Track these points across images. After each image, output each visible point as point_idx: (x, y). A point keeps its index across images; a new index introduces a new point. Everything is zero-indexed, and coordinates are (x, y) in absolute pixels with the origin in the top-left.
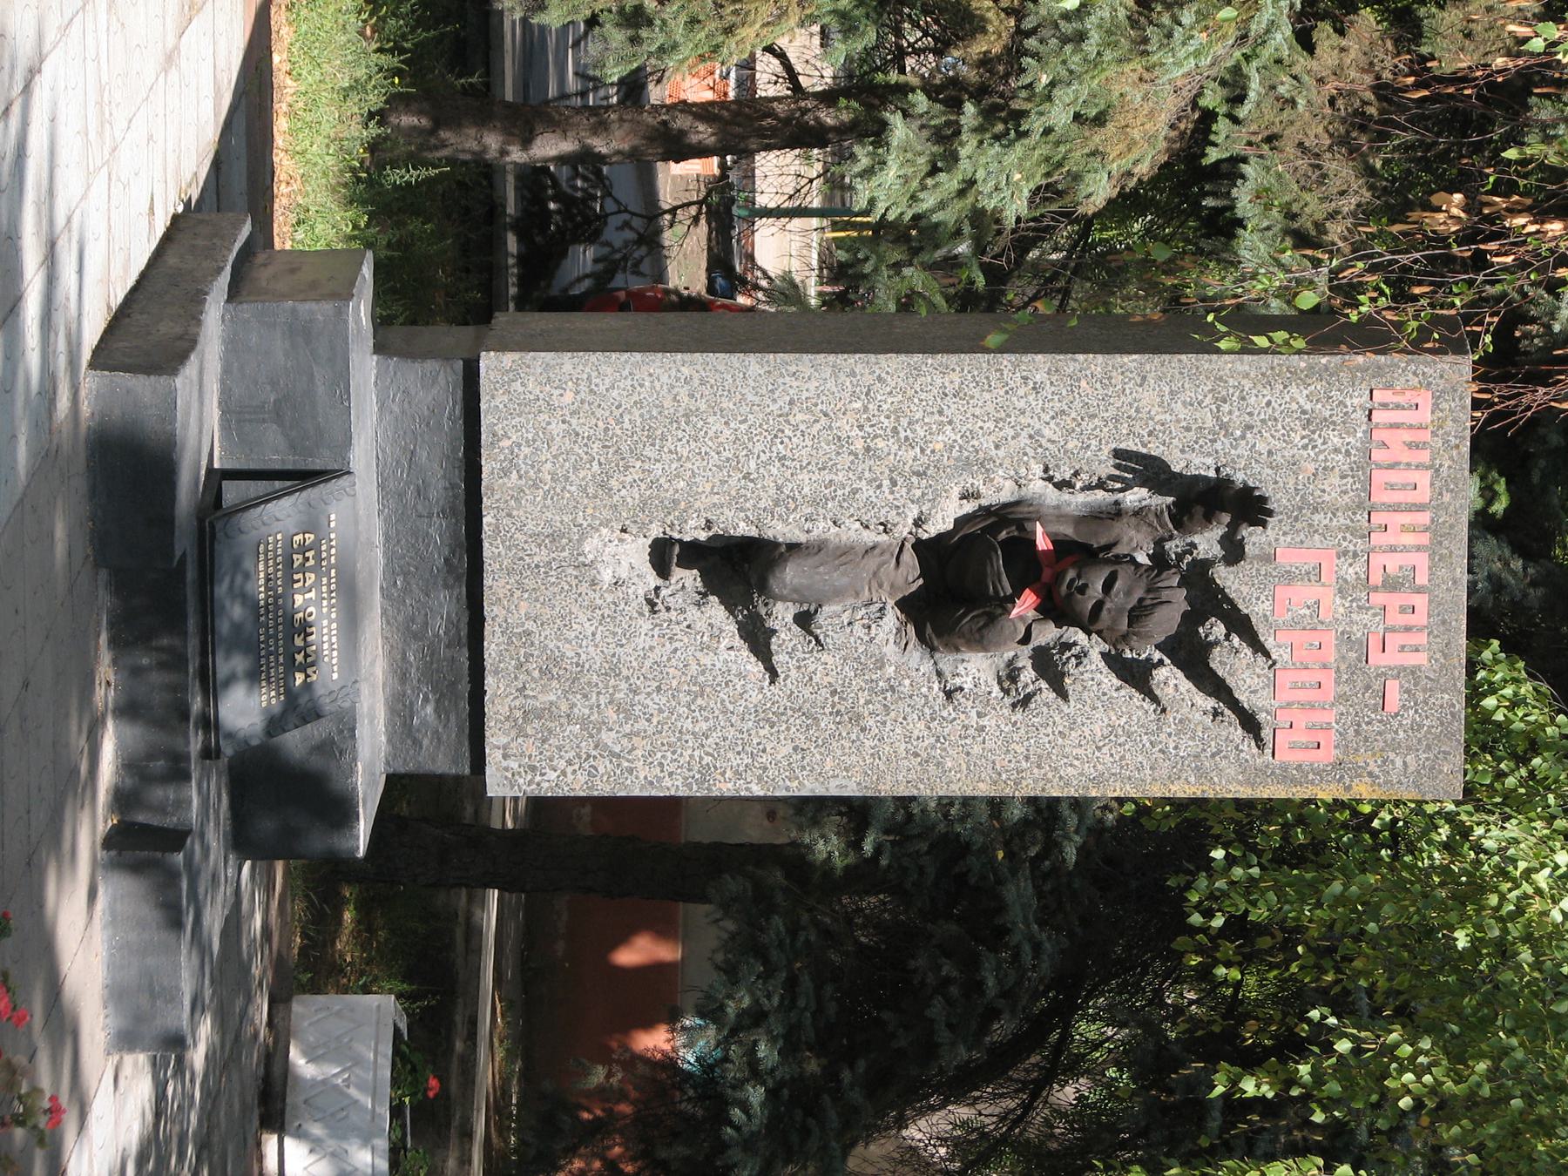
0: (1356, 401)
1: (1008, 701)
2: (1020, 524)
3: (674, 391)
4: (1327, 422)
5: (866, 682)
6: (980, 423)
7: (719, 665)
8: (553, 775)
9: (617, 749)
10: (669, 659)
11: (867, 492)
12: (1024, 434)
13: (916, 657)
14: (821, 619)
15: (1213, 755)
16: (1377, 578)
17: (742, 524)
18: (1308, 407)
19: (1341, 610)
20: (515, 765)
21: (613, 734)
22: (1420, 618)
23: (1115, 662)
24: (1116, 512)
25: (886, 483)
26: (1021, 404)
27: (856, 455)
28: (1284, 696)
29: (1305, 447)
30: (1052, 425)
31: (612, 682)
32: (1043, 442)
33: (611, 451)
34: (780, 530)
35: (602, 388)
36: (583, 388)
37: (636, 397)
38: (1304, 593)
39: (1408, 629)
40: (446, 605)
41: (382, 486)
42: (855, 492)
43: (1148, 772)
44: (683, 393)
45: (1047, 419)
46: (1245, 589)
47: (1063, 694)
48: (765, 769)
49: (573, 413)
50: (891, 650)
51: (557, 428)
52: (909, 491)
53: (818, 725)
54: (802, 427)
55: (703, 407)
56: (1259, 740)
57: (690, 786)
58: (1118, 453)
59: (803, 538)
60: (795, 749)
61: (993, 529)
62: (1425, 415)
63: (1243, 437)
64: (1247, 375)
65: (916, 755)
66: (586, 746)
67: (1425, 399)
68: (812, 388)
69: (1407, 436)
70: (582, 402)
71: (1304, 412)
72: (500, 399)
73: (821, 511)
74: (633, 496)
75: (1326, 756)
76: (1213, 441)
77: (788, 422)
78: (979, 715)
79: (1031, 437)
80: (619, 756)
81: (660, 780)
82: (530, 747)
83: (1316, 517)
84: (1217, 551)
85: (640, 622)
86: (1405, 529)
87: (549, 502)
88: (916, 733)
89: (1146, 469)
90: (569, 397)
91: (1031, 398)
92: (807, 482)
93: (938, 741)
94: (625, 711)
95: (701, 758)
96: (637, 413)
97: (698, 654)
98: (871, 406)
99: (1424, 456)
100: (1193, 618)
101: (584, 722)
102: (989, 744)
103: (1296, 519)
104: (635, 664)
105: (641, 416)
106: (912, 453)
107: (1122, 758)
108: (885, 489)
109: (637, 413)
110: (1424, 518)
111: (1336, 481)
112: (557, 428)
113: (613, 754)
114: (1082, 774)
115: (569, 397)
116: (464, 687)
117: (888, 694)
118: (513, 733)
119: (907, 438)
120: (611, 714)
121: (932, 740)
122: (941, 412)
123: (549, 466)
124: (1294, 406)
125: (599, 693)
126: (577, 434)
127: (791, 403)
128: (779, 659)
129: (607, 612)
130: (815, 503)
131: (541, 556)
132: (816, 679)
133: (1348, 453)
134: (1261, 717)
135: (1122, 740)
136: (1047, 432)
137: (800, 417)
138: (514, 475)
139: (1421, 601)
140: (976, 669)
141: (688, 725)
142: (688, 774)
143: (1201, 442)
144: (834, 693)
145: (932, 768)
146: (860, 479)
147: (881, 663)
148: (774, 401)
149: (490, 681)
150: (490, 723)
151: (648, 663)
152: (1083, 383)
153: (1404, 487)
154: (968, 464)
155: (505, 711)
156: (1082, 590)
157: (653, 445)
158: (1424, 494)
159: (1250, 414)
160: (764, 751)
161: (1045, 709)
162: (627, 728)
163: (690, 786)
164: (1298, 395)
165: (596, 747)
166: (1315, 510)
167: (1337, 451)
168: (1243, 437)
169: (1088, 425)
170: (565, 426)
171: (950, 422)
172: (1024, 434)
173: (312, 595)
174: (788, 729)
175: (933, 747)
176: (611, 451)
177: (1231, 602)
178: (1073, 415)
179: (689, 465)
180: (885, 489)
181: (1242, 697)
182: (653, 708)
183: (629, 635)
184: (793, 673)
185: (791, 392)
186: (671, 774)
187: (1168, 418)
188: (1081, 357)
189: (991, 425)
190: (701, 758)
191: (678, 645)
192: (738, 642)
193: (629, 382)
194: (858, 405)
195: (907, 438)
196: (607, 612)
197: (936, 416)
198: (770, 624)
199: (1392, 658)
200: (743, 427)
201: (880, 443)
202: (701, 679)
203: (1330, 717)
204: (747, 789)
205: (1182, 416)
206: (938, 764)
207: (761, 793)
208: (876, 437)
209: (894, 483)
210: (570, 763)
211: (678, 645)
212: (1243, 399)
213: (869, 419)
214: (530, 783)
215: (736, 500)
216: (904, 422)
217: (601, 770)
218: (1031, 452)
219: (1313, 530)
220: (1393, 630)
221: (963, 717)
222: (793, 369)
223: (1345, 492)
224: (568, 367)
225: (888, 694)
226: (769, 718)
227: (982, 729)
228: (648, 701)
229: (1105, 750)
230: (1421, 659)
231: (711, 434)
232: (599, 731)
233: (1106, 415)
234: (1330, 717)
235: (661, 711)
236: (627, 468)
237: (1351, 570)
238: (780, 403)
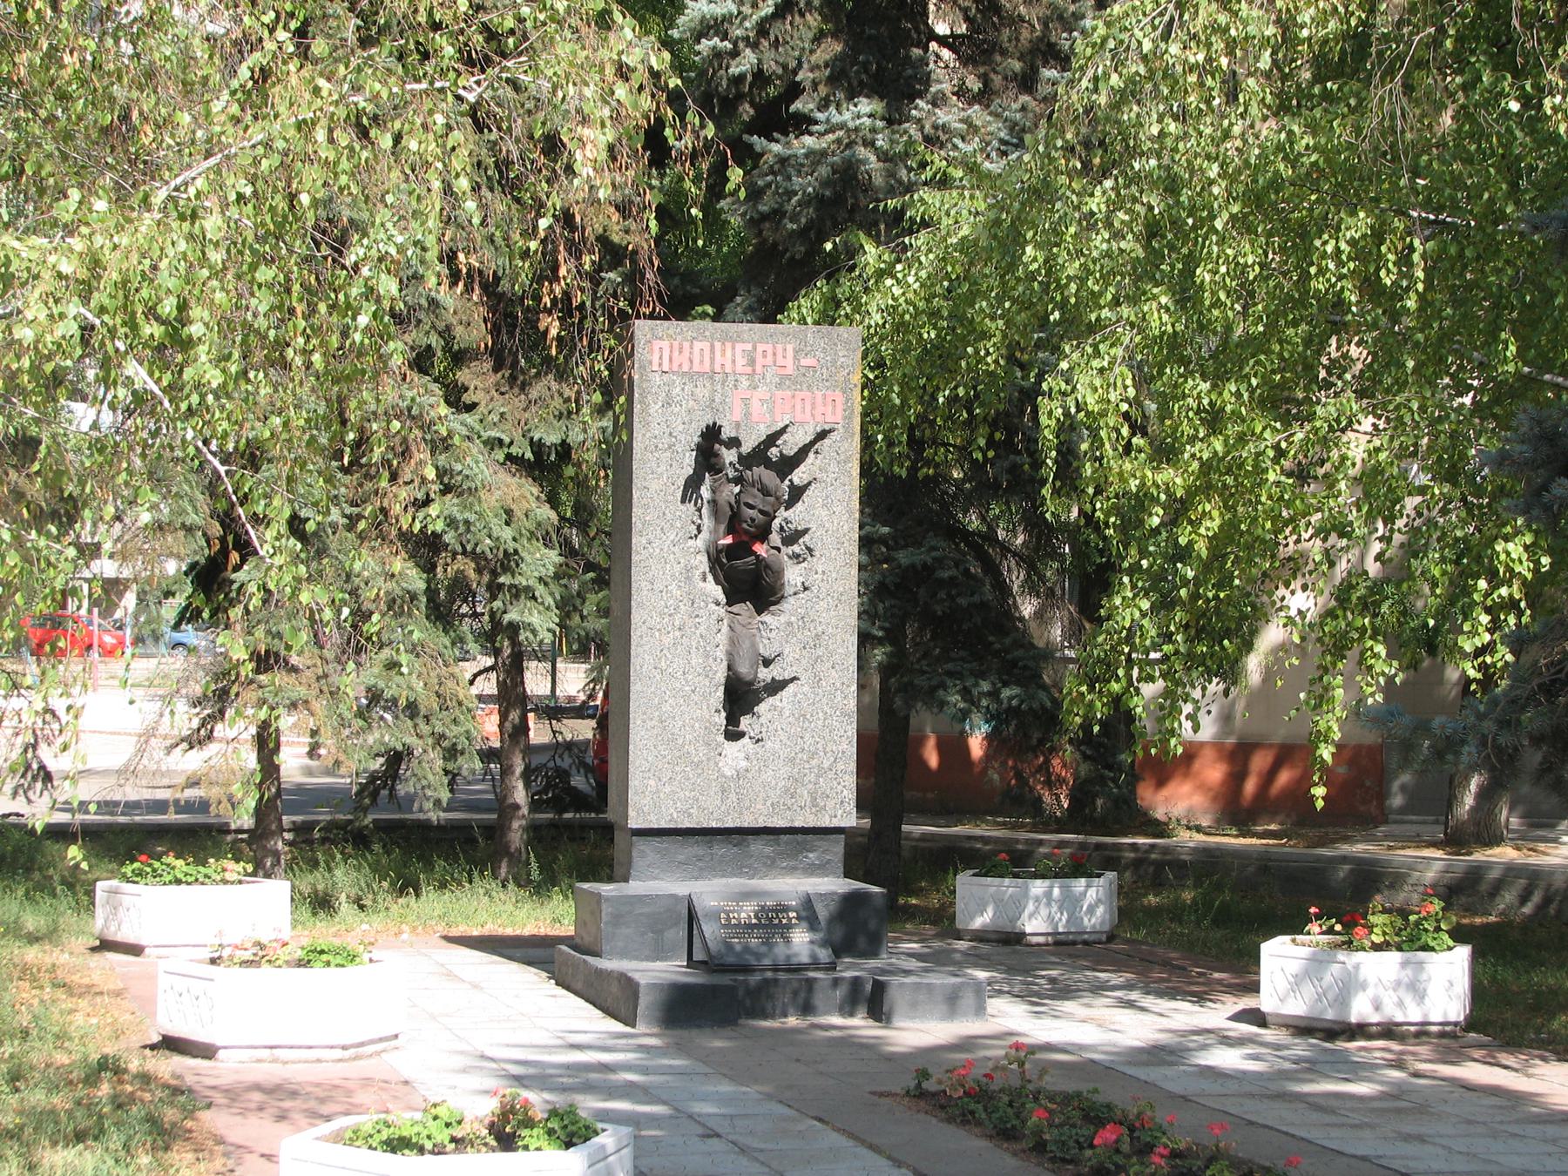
2: (719, 552)
11: (702, 629)
14: (766, 654)
16: (749, 370)
22: (769, 348)
23: (790, 504)
24: (713, 503)
34: (721, 675)
38: (756, 408)
40: (757, 846)
41: (697, 879)
44: (650, 724)
47: (806, 531)
50: (783, 619)
51: (667, 789)
56: (830, 431)
58: (683, 501)
59: (725, 663)
61: (721, 565)
62: (665, 344)
66: (831, 775)
67: (657, 344)
69: (676, 353)
72: (652, 817)
74: (703, 750)
75: (839, 396)
82: (830, 804)
84: (734, 451)
86: (723, 355)
89: (691, 487)
90: (652, 782)
92: (696, 660)
94: (813, 755)
99: (686, 345)
100: (768, 464)
101: (818, 776)
110: (718, 345)
112: (667, 789)
115: (652, 782)
116: (800, 837)
120: (814, 762)
130: (707, 656)
131: (733, 797)
134: (819, 429)
140: (793, 575)
147: (790, 624)
149: (797, 824)
150: (819, 824)
154: (688, 578)
156: (753, 520)
158: (706, 345)
164: (654, 408)
169: (669, 516)
192: (778, 697)
198: (769, 680)
199: (789, 362)
203: (819, 394)
219: (723, 402)
230: (790, 348)
234: (819, 394)
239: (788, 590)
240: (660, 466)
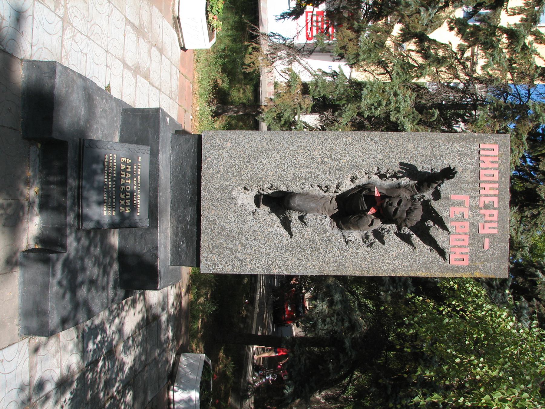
0: (475, 148)
1: (365, 245)
2: (369, 189)
4: (466, 155)
5: (321, 237)
11: (322, 175)
12: (371, 157)
13: (336, 231)
14: (307, 217)
15: (430, 263)
16: (482, 205)
17: (282, 186)
18: (460, 149)
19: (471, 215)
20: (209, 263)
21: (240, 254)
22: (495, 218)
23: (398, 234)
24: (399, 186)
25: (328, 172)
26: (371, 148)
27: (318, 164)
28: (453, 243)
29: (459, 163)
32: (377, 160)
34: (294, 188)
37: (250, 145)
38: (458, 210)
39: (491, 222)
40: (190, 213)
41: (172, 174)
42: (318, 175)
43: (410, 268)
44: (264, 143)
45: (379, 152)
46: (441, 208)
47: (383, 242)
50: (328, 227)
51: (225, 154)
53: (305, 252)
54: (302, 154)
55: (271, 148)
56: (445, 258)
58: (401, 164)
59: (301, 191)
60: (298, 259)
61: (361, 192)
62: (496, 153)
63: (440, 159)
64: (441, 139)
65: (336, 262)
66: (232, 257)
67: (496, 147)
69: (491, 159)
71: (459, 151)
72: (208, 145)
74: (248, 176)
75: (466, 263)
76: (431, 160)
77: (297, 153)
78: (357, 249)
79: (374, 158)
80: (242, 261)
81: (255, 269)
83: (463, 185)
84: (431, 197)
87: (222, 178)
88: (336, 254)
89: (410, 170)
90: (229, 145)
92: (303, 172)
93: (343, 257)
94: (244, 246)
96: (250, 150)
99: (496, 166)
100: (424, 219)
101: (231, 250)
102: (359, 259)
103: (457, 185)
106: (336, 163)
107: (402, 263)
108: (327, 174)
109: (250, 150)
110: (496, 186)
111: (469, 173)
112: (225, 154)
113: (240, 260)
114: (389, 269)
116: (195, 238)
118: (209, 252)
119: (334, 158)
120: (240, 247)
121: (341, 257)
122: (345, 150)
123: (222, 166)
124: (456, 149)
128: (293, 230)
129: (239, 214)
130: (305, 179)
131: (219, 195)
132: (305, 236)
133: (472, 165)
134: (446, 250)
136: (378, 156)
137: (301, 151)
138: (212, 169)
139: (495, 213)
140: (355, 235)
144: (310, 241)
145: (341, 266)
147: (325, 231)
148: (293, 146)
149: (202, 235)
150: (202, 249)
151: (251, 231)
152: (390, 141)
153: (490, 175)
155: (206, 245)
156: (391, 204)
158: (496, 178)
159: (442, 152)
162: (245, 252)
163: (264, 271)
164: (457, 146)
166: (462, 183)
167: (469, 164)
168: (440, 159)
171: (348, 153)
172: (371, 157)
174: (296, 253)
175: (342, 259)
177: (436, 212)
180: (327, 174)
181: (440, 244)
182: (253, 245)
183: (246, 221)
184: (298, 234)
186: (258, 267)
188: (389, 133)
189: (361, 154)
192: (280, 225)
193: (248, 140)
194: (319, 147)
195: (334, 158)
196: (239, 214)
198: (291, 219)
199: (487, 231)
201: (326, 160)
206: (343, 265)
207: (287, 274)
208: (325, 157)
209: (330, 173)
210: (226, 263)
212: (440, 147)
215: (281, 178)
216: (334, 153)
217: (236, 265)
218: (374, 163)
220: (487, 222)
222: (299, 136)
223: (472, 177)
224: (229, 135)
226: (290, 249)
228: (251, 243)
229: (396, 261)
230: (495, 231)
231: (273, 156)
232: (236, 252)
234: (467, 250)
235: (256, 246)
237: (474, 203)
239: (346, 233)
240: (425, 149)
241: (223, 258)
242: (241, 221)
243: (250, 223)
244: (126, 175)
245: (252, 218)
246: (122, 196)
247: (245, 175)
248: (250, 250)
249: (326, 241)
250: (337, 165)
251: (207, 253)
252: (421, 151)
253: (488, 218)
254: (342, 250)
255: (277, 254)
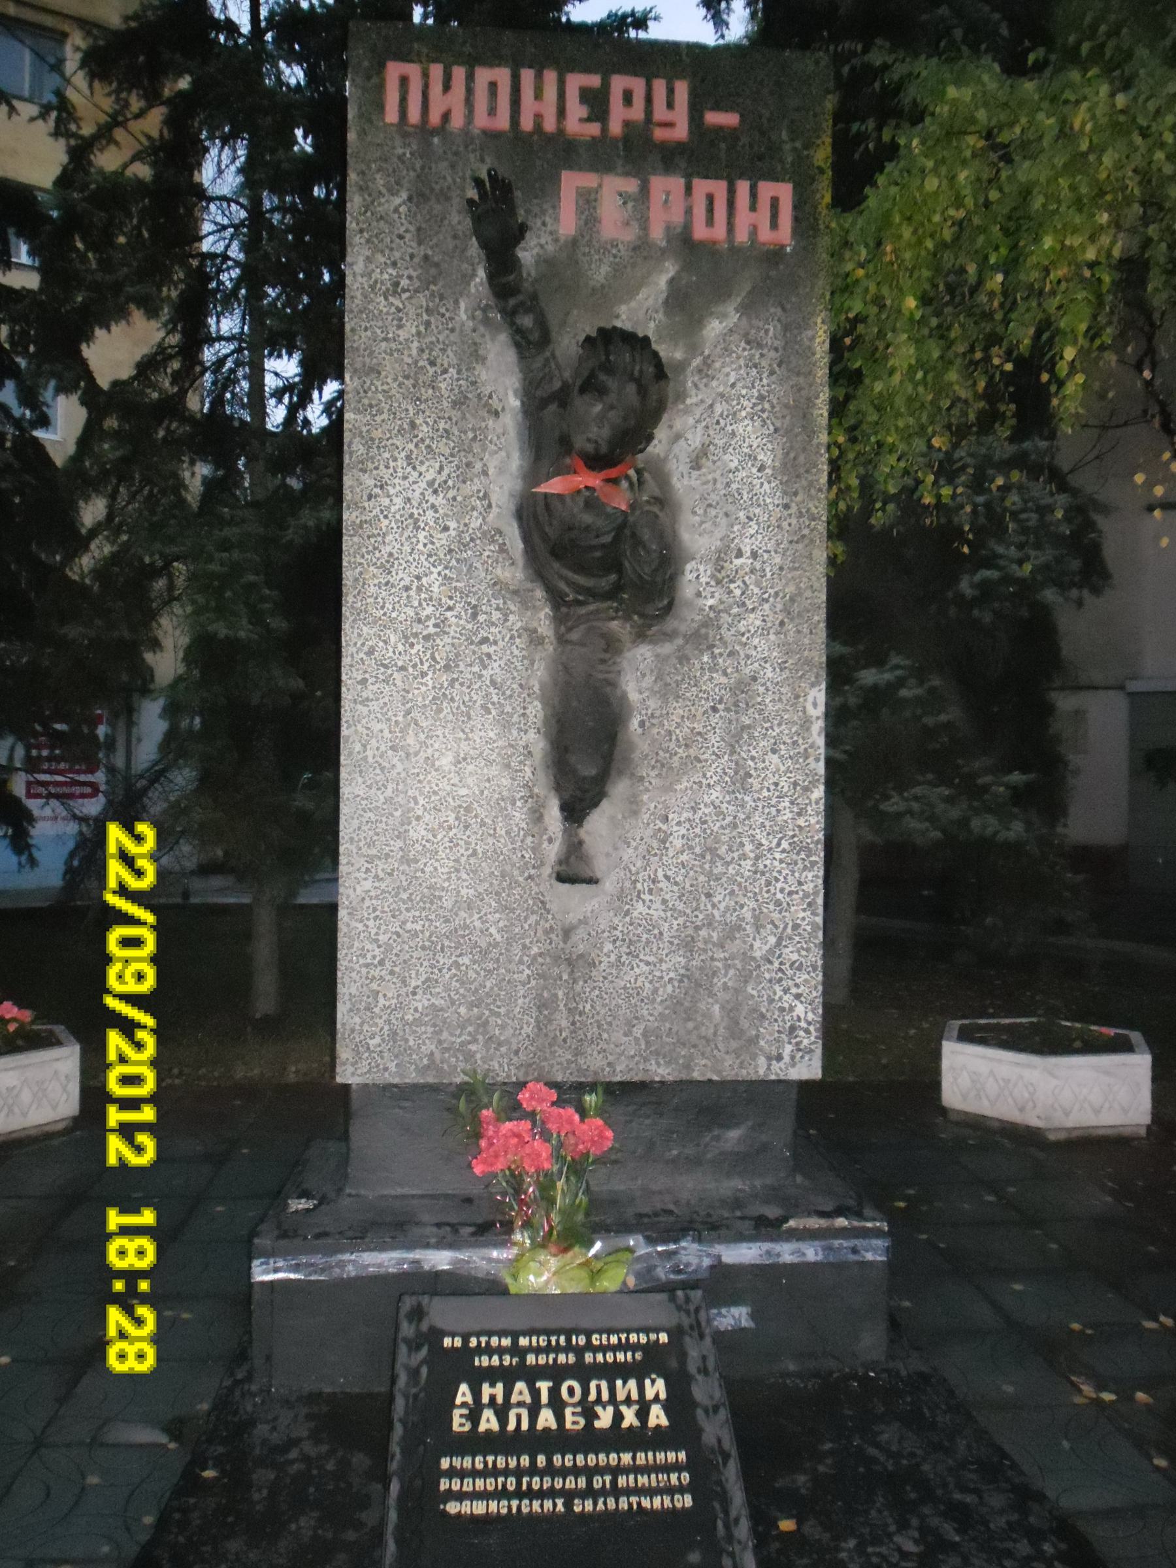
3: (381, 875)
6: (420, 546)
7: (683, 831)
8: (800, 1009)
9: (772, 940)
10: (676, 884)
11: (494, 669)
16: (594, 129)
20: (788, 1049)
21: (757, 944)
22: (637, 85)
25: (485, 648)
26: (398, 501)
27: (453, 681)
30: (423, 469)
31: (701, 945)
33: (447, 943)
35: (377, 951)
36: (376, 973)
39: (649, 99)
42: (493, 683)
45: (416, 474)
48: (795, 784)
49: (404, 982)
51: (421, 1002)
52: (493, 624)
53: (749, 727)
57: (813, 864)
60: (774, 751)
63: (437, 265)
68: (380, 726)
70: (392, 973)
73: (515, 719)
75: (784, 192)
77: (416, 754)
78: (739, 554)
80: (780, 939)
81: (806, 895)
85: (635, 914)
86: (538, 95)
87: (502, 1010)
91: (392, 491)
93: (767, 601)
95: (784, 851)
97: (671, 854)
98: (400, 664)
99: (459, 73)
104: (681, 920)
105: (408, 910)
117: (717, 651)
119: (436, 625)
120: (735, 947)
121: (766, 606)
122: (407, 589)
123: (463, 1010)
124: (403, 209)
125: (712, 959)
126: (428, 980)
127: (394, 748)
129: (625, 949)
135: (767, 406)
136: (429, 477)
137: (411, 740)
138: (473, 1047)
139: (618, 83)
141: (747, 864)
142: (800, 865)
143: (443, 310)
145: (796, 608)
146: (480, 676)
151: (681, 907)
155: (729, 1061)
157: (440, 898)
158: (502, 75)
160: (776, 784)
161: (734, 486)
162: (749, 929)
165: (771, 962)
170: (420, 991)
171: (418, 578)
172: (432, 499)
173: (544, 1386)
174: (753, 758)
176: (447, 943)
178: (411, 446)
179: (463, 860)
180: (492, 650)
185: (383, 748)
186: (800, 883)
187: (416, 344)
189: (422, 535)
190: (784, 851)
191: (660, 874)
193: (371, 923)
195: (436, 625)
196: (625, 949)
197: (412, 593)
200: (421, 802)
202: (698, 850)
204: (817, 803)
205: (414, 331)
207: (822, 788)
208: (433, 658)
209: (485, 640)
210: (786, 991)
211: (660, 874)
213: (415, 666)
214: (807, 1031)
217: (795, 957)
221: (741, 573)
222: (358, 747)
225: (717, 651)
226: (740, 780)
227: (754, 555)
228: (722, 906)
230: (682, 90)
232: (754, 959)
233: (411, 412)
235: (732, 893)
236: (466, 927)
238: (395, 761)
241: (771, 1001)
242: (648, 942)
243: (657, 912)
244: (520, 1404)
245: (640, 907)
246: (605, 1419)
247: (493, 930)
248: (747, 913)
249: (713, 657)
250: (458, 617)
251: (754, 1057)
252: (410, 329)
253: (637, 112)
254: (744, 604)
255: (758, 818)
